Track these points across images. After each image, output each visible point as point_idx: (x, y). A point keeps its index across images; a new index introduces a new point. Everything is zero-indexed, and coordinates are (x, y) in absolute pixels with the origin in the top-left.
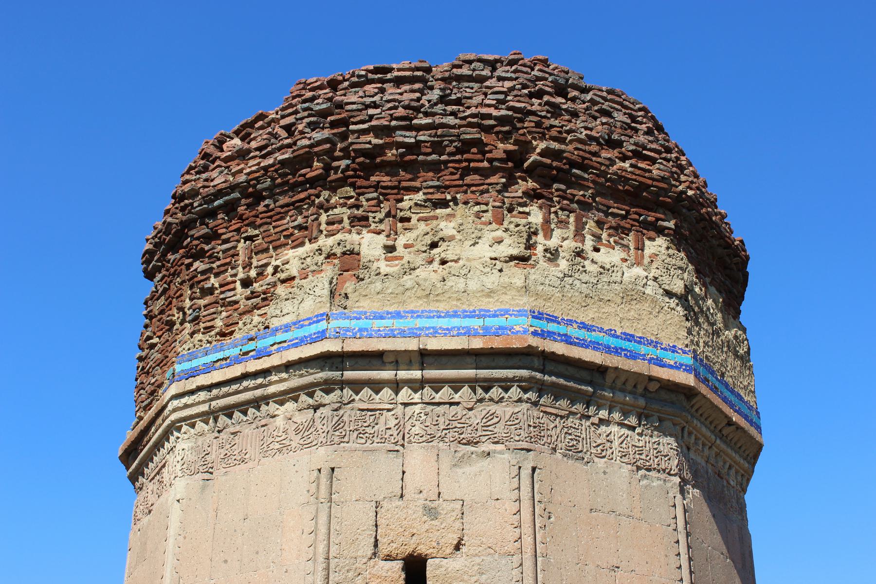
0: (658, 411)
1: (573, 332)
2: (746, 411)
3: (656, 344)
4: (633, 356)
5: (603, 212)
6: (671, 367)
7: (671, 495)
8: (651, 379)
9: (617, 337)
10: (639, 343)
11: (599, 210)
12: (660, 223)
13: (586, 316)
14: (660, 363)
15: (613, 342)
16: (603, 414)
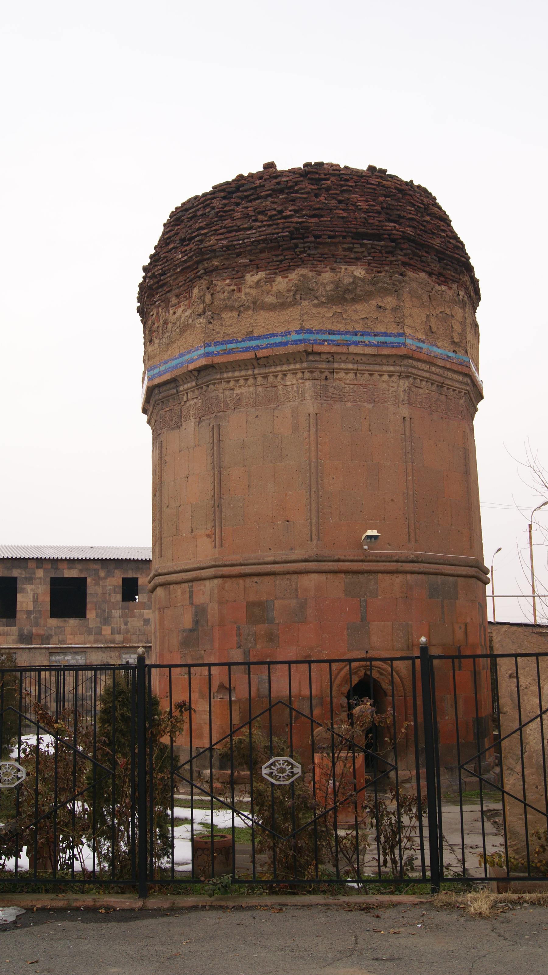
0: (203, 384)
1: (163, 368)
2: (278, 339)
3: (189, 352)
4: (182, 364)
5: (177, 288)
6: (196, 359)
7: (211, 425)
8: (191, 371)
9: (176, 359)
10: (184, 355)
11: (175, 289)
12: (199, 274)
13: (166, 357)
14: (192, 361)
15: (175, 363)
16: (185, 399)
